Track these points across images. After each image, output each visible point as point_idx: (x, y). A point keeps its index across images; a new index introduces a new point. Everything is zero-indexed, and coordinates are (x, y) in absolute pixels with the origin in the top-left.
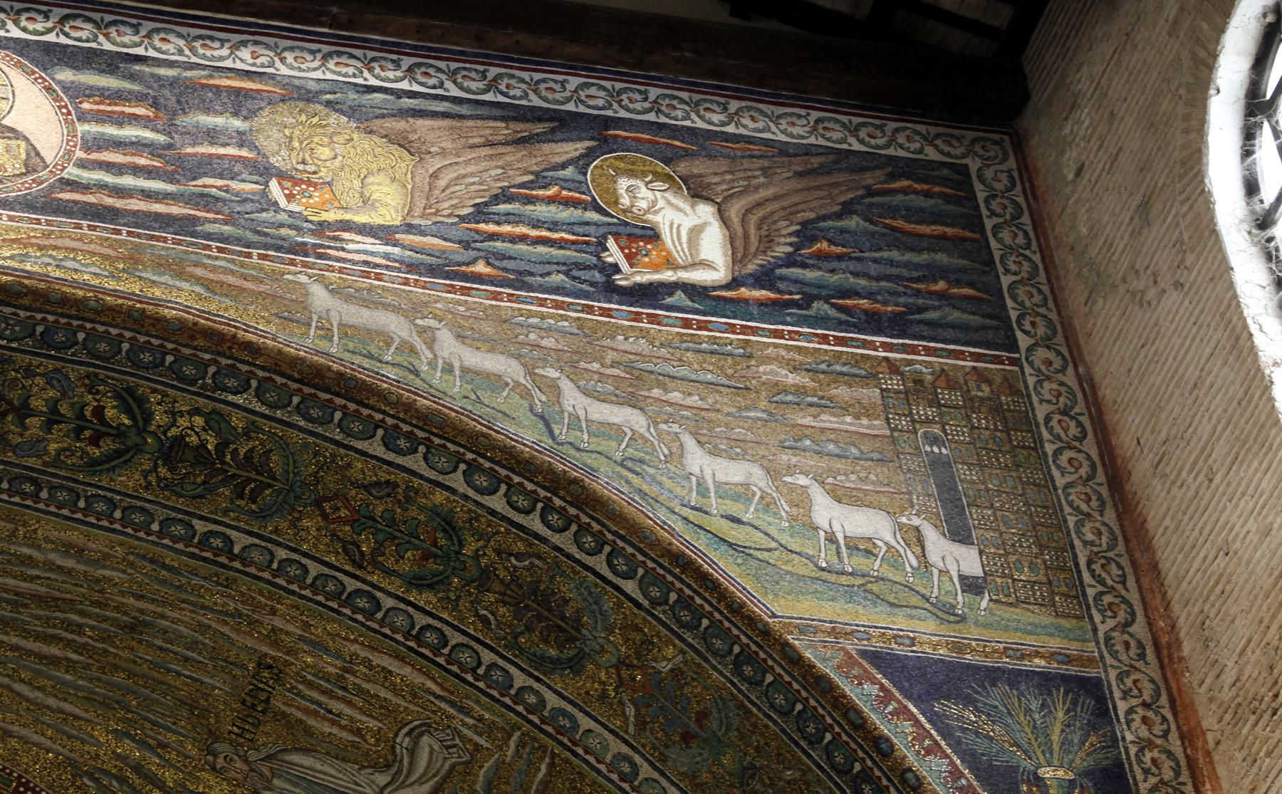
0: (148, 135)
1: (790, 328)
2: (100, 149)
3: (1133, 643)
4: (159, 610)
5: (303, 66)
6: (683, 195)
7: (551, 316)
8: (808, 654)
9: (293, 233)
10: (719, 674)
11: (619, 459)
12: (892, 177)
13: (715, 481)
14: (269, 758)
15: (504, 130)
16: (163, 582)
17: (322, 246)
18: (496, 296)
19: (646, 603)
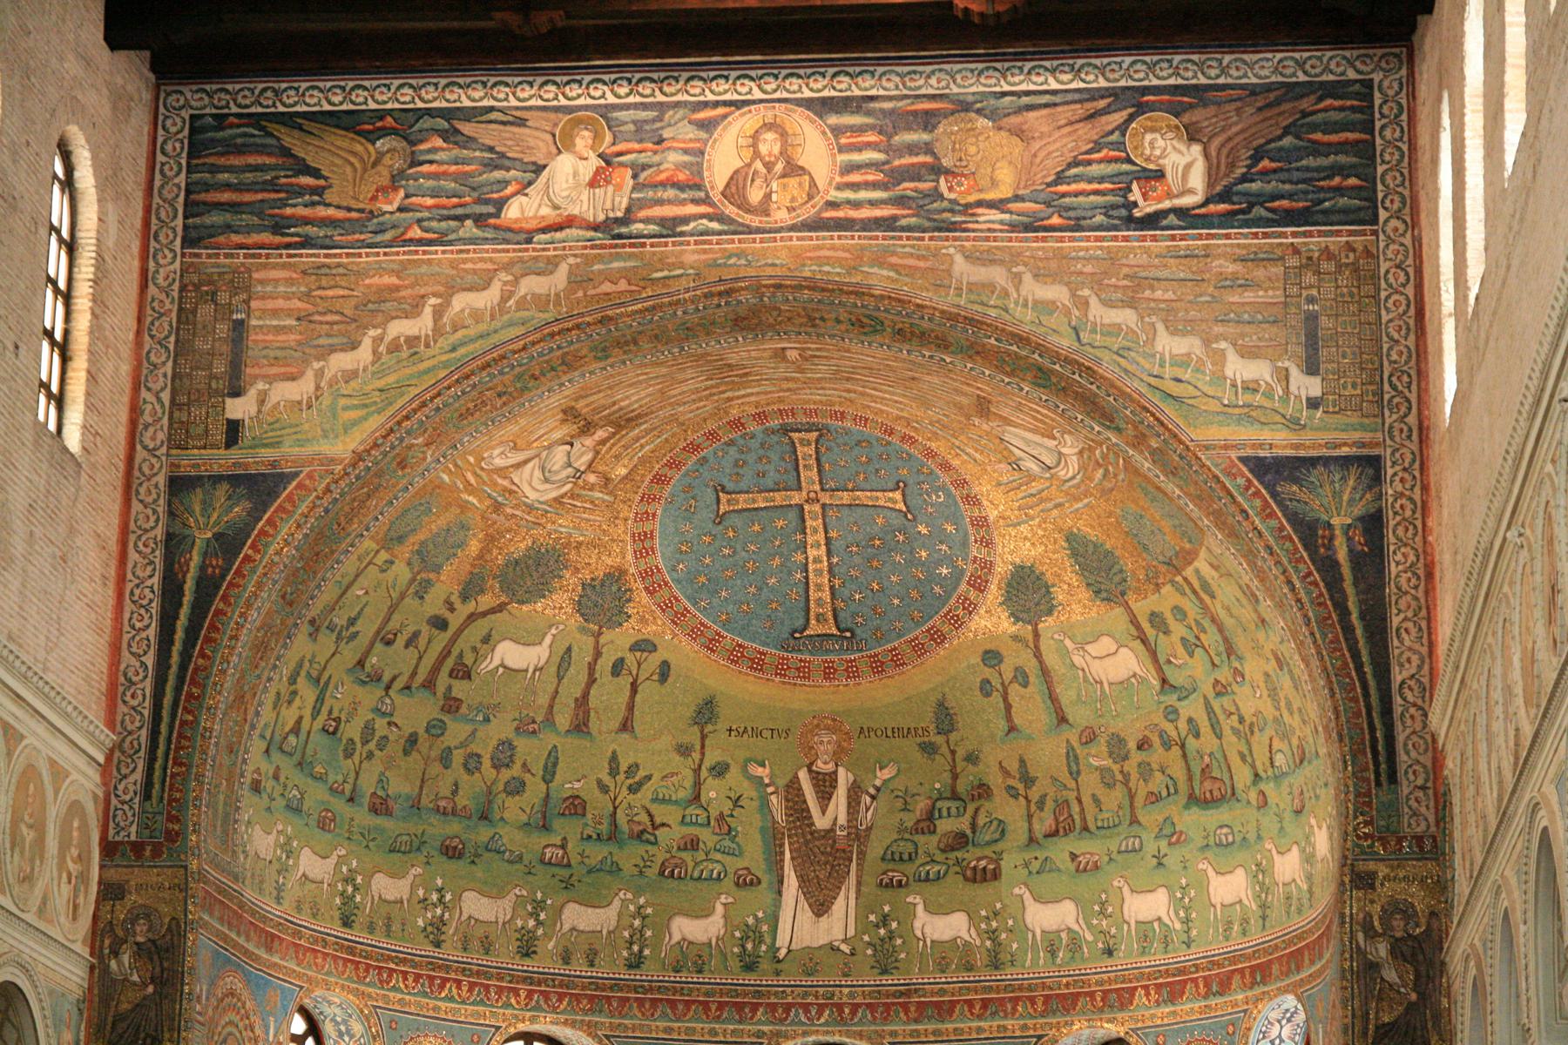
15: (1079, 110)
18: (1061, 240)
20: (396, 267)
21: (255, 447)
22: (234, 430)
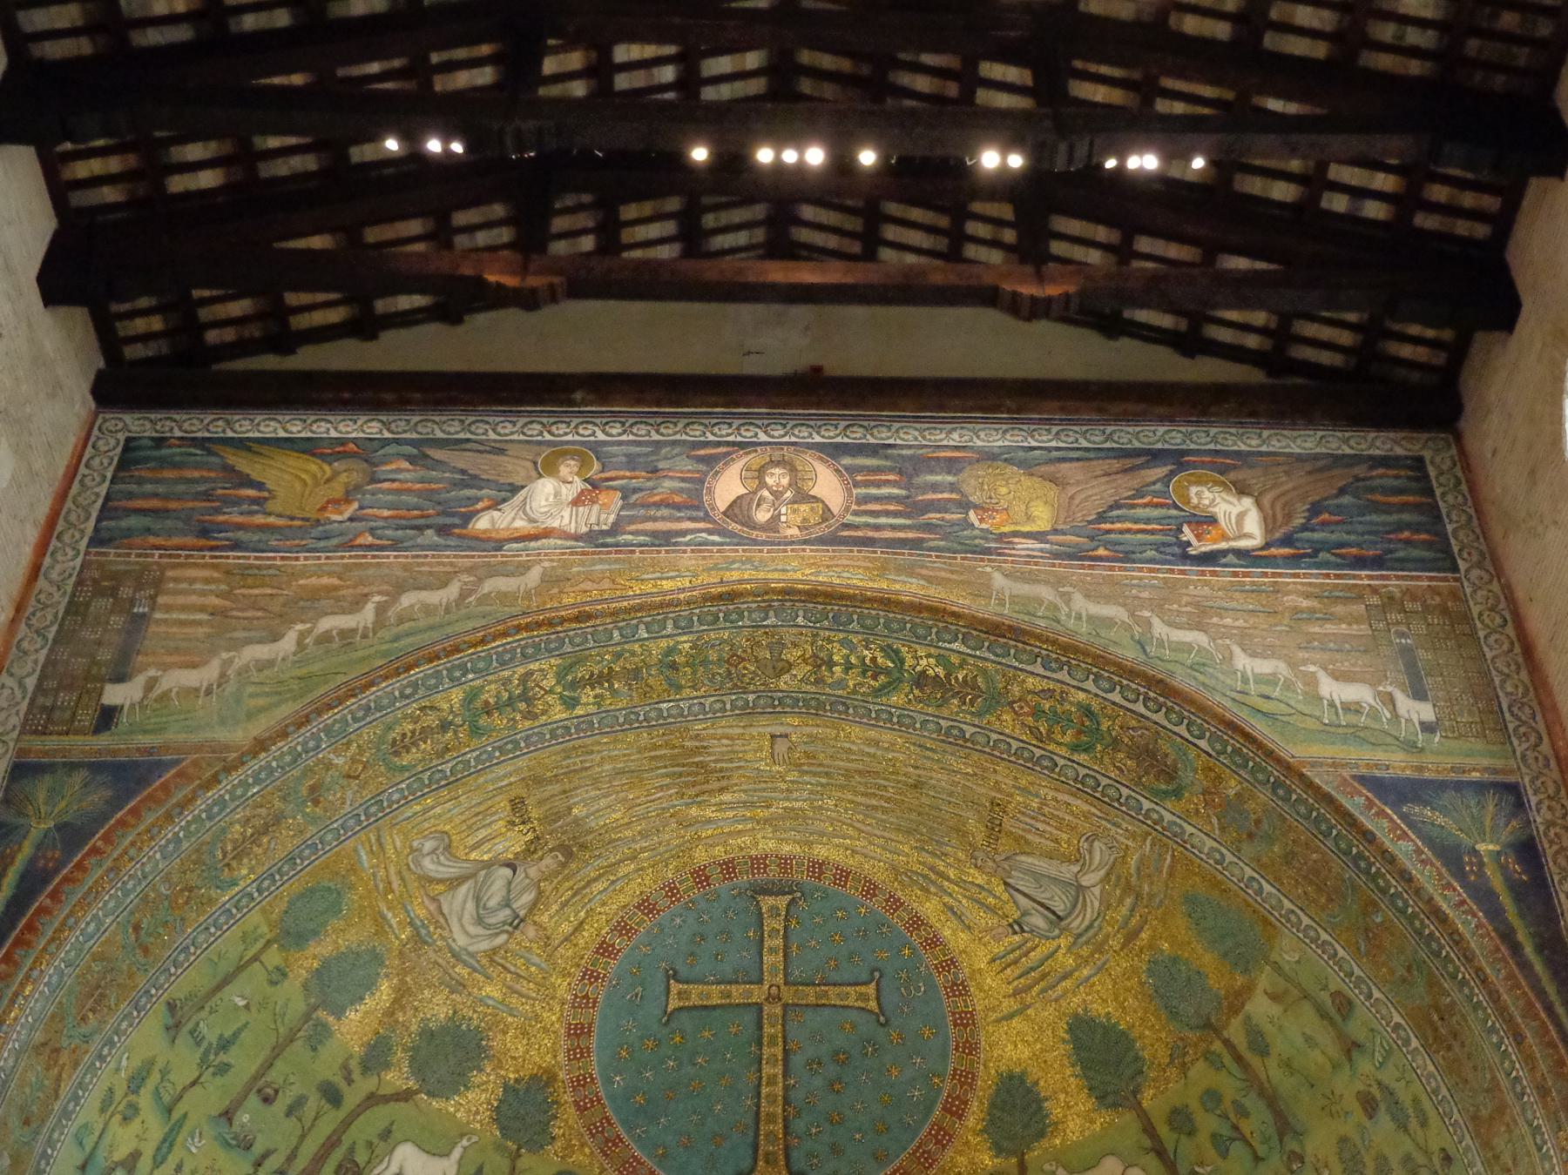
0: (896, 491)
2: (866, 503)
3: (1540, 758)
7: (1146, 578)
8: (1317, 781)
9: (982, 542)
10: (1264, 796)
12: (1372, 468)
14: (1007, 859)
15: (1117, 464)
16: (928, 758)
18: (1111, 569)
19: (1213, 753)
20: (337, 569)
21: (132, 732)
22: (108, 717)
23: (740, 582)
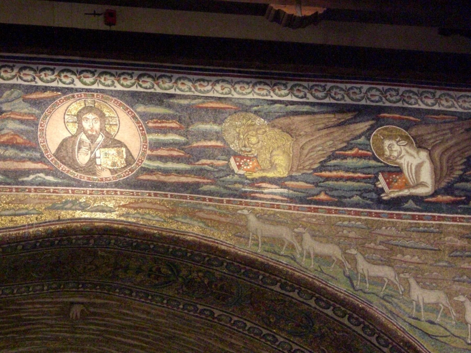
0: (177, 138)
1: (460, 216)
4: (182, 333)
5: (244, 92)
6: (413, 147)
7: (354, 219)
9: (240, 186)
11: (381, 296)
13: (424, 303)
15: (333, 119)
17: (253, 192)
18: (329, 211)
23: (74, 220)
